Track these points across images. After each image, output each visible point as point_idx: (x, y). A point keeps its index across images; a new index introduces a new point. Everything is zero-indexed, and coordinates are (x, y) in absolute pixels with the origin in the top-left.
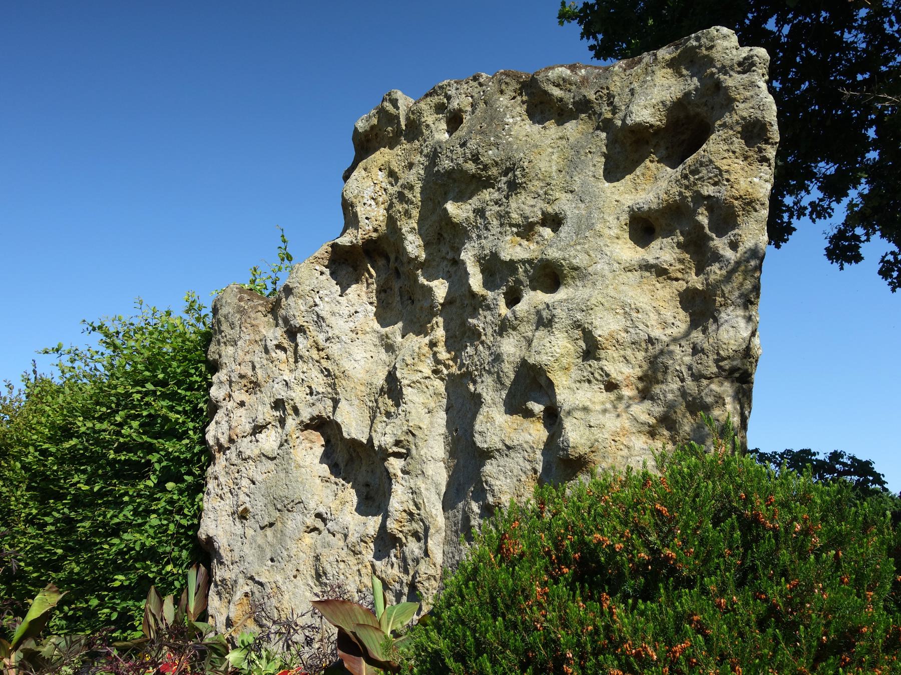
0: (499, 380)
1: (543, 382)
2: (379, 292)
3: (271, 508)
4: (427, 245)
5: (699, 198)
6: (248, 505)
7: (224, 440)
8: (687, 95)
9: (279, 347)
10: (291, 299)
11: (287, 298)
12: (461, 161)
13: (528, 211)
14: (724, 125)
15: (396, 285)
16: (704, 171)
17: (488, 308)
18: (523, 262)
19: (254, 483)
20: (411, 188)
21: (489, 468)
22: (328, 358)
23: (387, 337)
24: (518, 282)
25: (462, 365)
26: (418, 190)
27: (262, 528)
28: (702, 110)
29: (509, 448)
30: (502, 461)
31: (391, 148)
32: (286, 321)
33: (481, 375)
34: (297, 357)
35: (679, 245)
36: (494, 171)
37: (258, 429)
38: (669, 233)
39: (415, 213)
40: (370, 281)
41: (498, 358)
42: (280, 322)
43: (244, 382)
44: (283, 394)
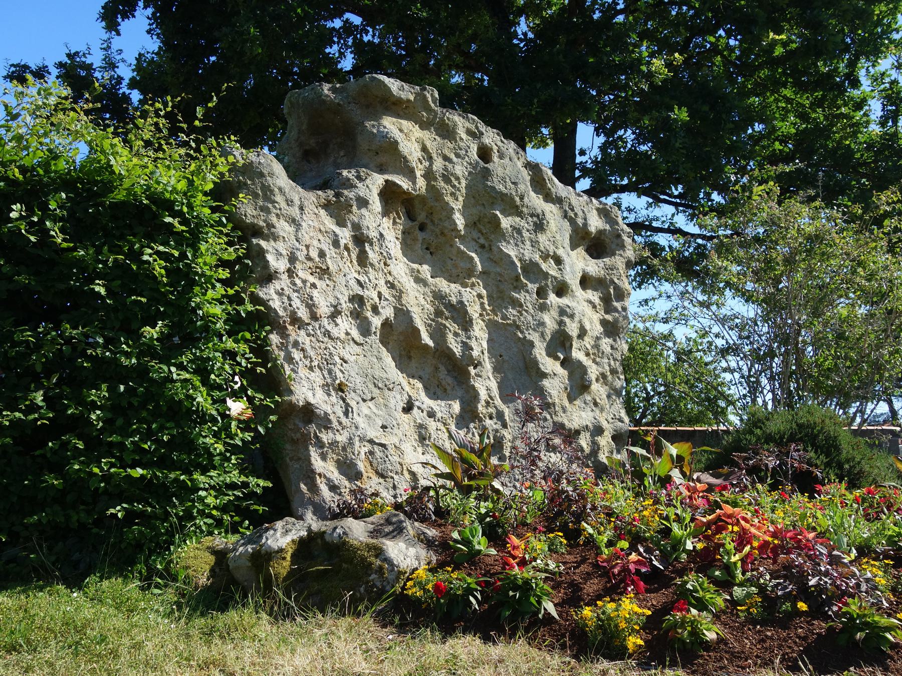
0: (542, 335)
1: (568, 345)
2: (403, 233)
3: (371, 386)
4: (466, 226)
5: (612, 282)
6: (343, 379)
7: (303, 313)
8: (605, 230)
9: (347, 248)
10: (364, 211)
11: (359, 208)
12: (514, 194)
13: (548, 248)
14: (621, 255)
15: (420, 236)
16: (615, 272)
17: (527, 291)
18: (552, 276)
19: (346, 362)
20: (458, 179)
21: (546, 383)
22: (390, 273)
23: (418, 271)
24: (546, 285)
25: (505, 317)
26: (464, 183)
27: (364, 400)
28: (607, 240)
29: (555, 374)
30: (551, 380)
31: (421, 128)
32: (357, 227)
33: (527, 329)
34: (363, 260)
35: (600, 298)
36: (525, 210)
37: (335, 314)
38: (595, 290)
39: (461, 199)
40: (398, 221)
41: (542, 324)
42: (349, 225)
43: (310, 264)
44: (359, 291)
